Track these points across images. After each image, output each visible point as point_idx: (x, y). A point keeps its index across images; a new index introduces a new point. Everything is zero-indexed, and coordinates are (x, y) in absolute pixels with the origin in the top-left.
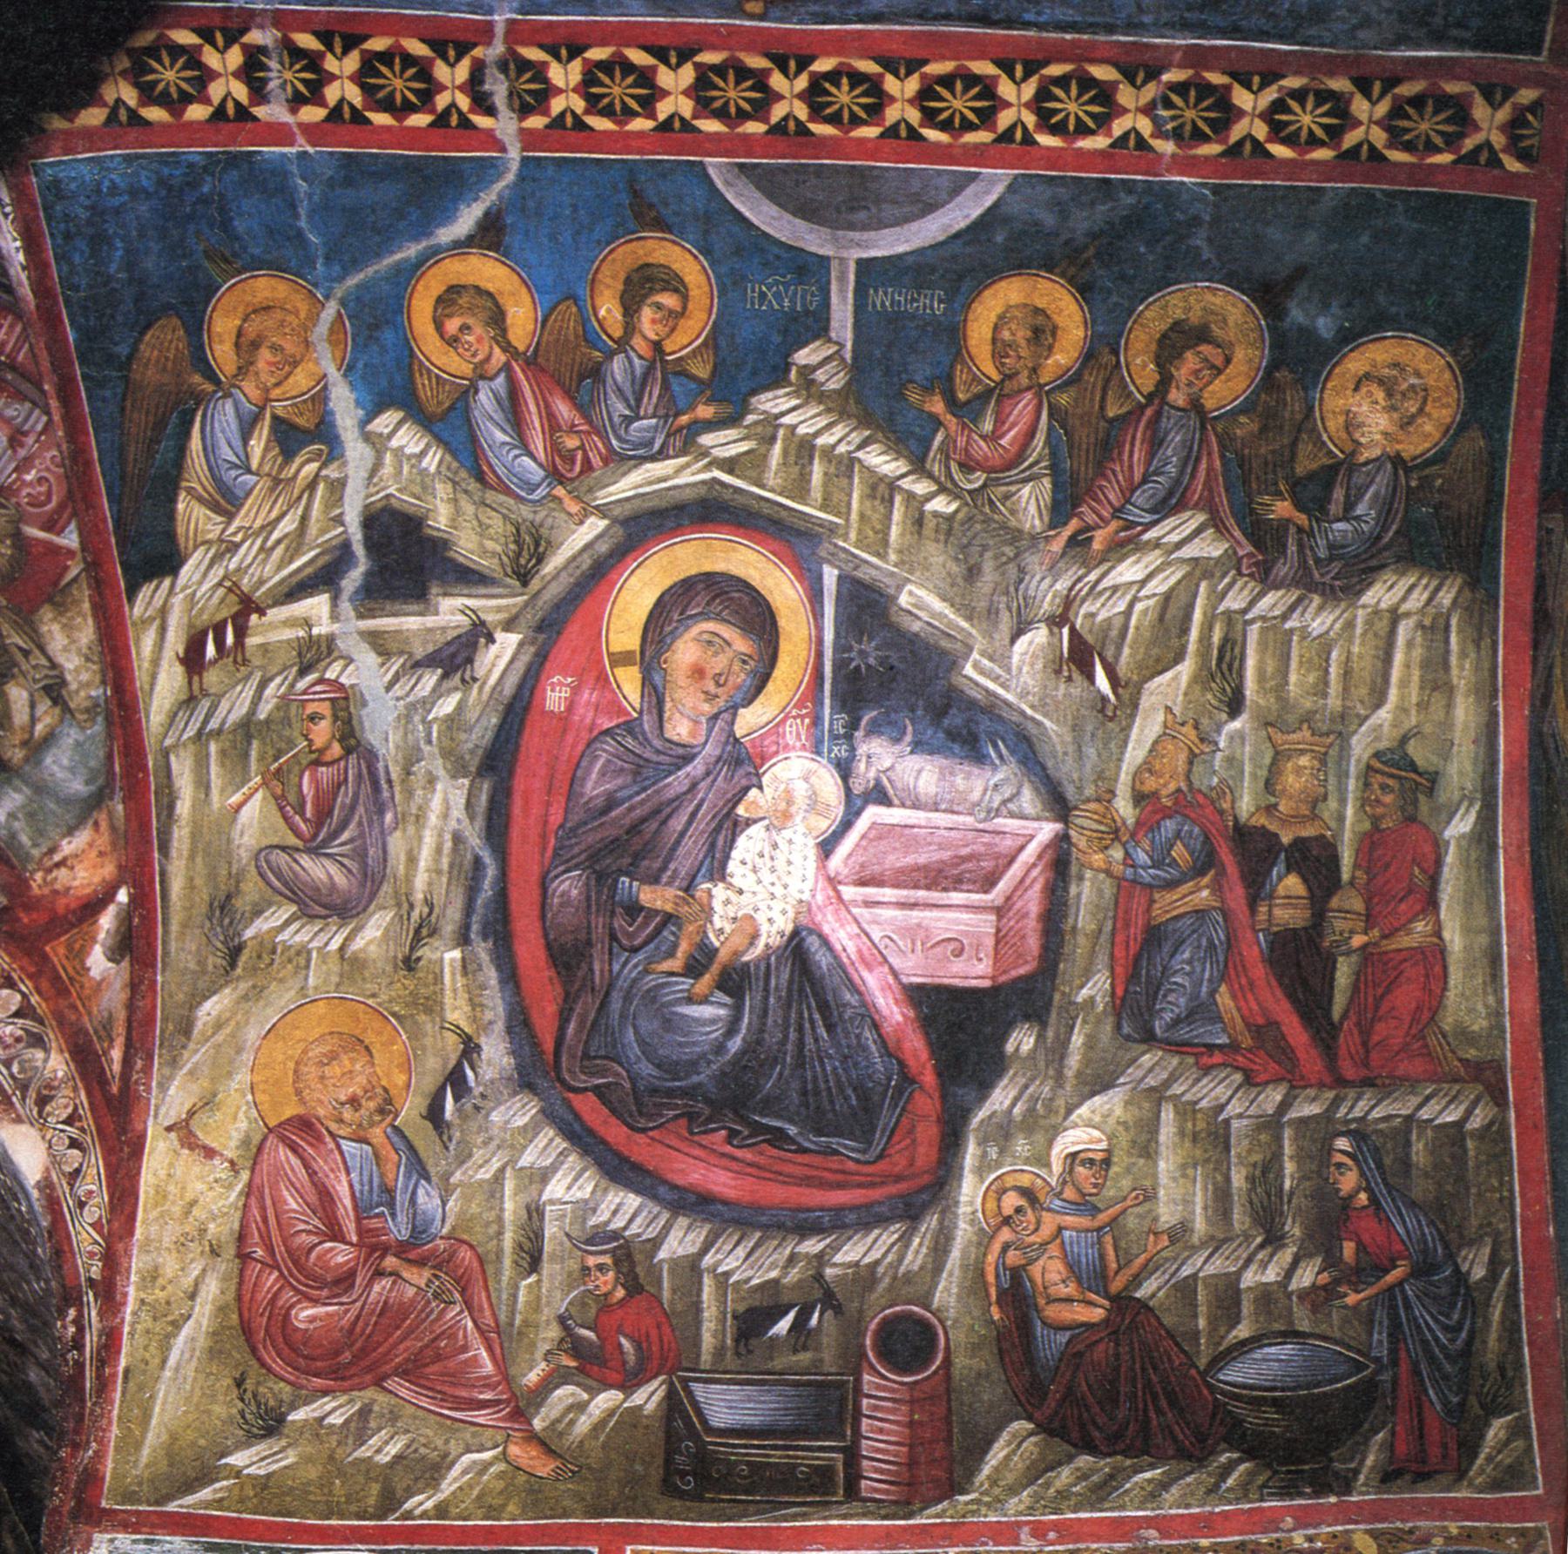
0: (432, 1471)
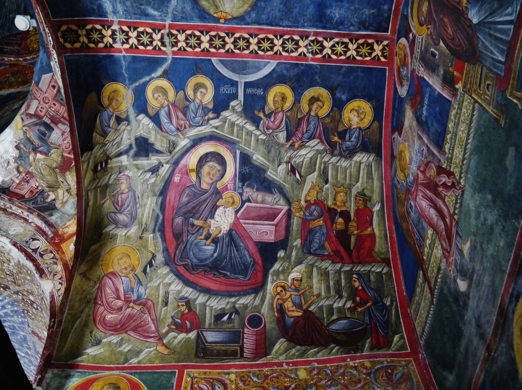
0: (138, 353)
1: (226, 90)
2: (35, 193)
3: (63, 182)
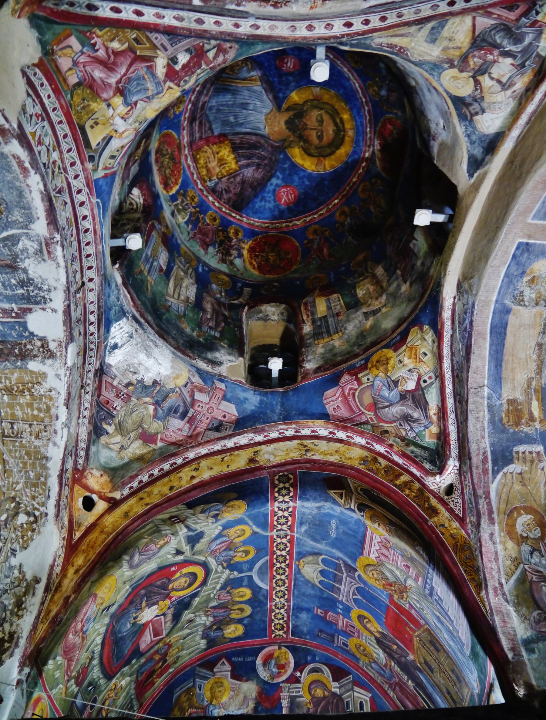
1: (245, 567)
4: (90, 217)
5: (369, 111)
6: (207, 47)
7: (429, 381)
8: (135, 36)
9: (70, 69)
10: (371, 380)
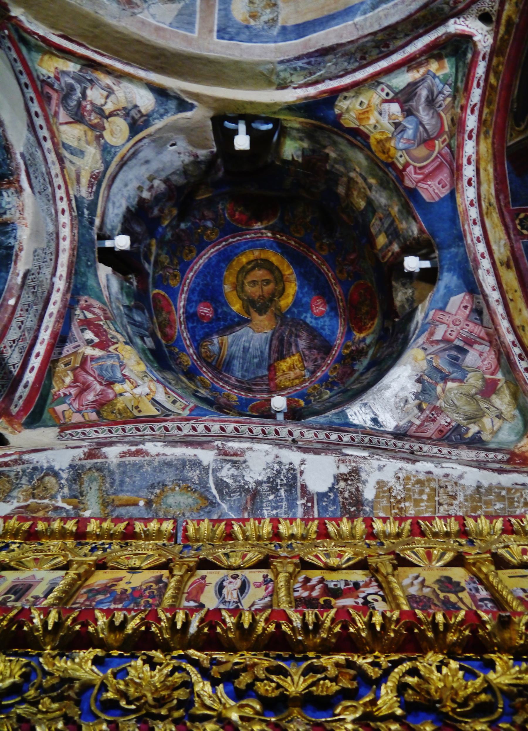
2: (445, 431)
3: (488, 409)
4: (223, 425)
5: (233, 238)
6: (82, 317)
7: (387, 90)
8: (63, 366)
9: (83, 416)
10: (400, 153)
